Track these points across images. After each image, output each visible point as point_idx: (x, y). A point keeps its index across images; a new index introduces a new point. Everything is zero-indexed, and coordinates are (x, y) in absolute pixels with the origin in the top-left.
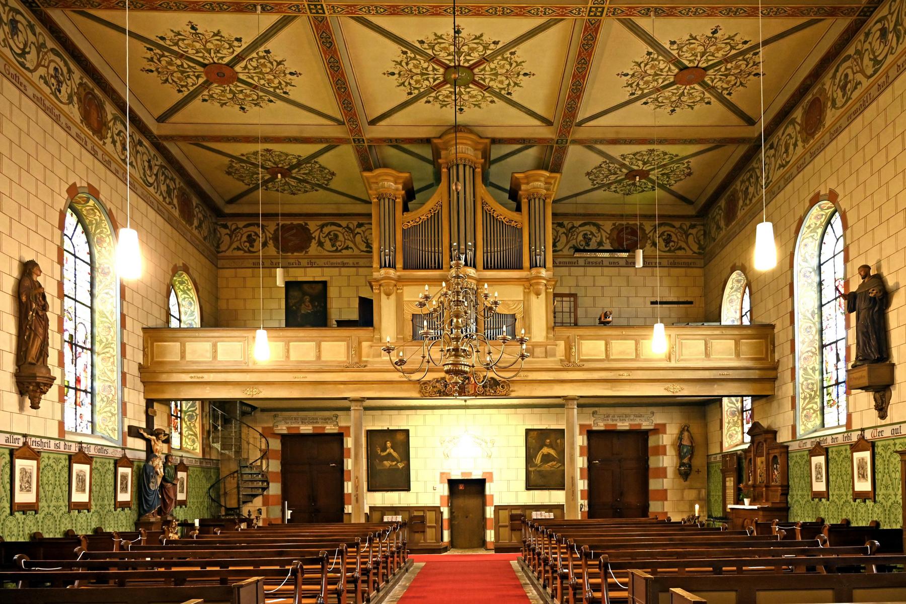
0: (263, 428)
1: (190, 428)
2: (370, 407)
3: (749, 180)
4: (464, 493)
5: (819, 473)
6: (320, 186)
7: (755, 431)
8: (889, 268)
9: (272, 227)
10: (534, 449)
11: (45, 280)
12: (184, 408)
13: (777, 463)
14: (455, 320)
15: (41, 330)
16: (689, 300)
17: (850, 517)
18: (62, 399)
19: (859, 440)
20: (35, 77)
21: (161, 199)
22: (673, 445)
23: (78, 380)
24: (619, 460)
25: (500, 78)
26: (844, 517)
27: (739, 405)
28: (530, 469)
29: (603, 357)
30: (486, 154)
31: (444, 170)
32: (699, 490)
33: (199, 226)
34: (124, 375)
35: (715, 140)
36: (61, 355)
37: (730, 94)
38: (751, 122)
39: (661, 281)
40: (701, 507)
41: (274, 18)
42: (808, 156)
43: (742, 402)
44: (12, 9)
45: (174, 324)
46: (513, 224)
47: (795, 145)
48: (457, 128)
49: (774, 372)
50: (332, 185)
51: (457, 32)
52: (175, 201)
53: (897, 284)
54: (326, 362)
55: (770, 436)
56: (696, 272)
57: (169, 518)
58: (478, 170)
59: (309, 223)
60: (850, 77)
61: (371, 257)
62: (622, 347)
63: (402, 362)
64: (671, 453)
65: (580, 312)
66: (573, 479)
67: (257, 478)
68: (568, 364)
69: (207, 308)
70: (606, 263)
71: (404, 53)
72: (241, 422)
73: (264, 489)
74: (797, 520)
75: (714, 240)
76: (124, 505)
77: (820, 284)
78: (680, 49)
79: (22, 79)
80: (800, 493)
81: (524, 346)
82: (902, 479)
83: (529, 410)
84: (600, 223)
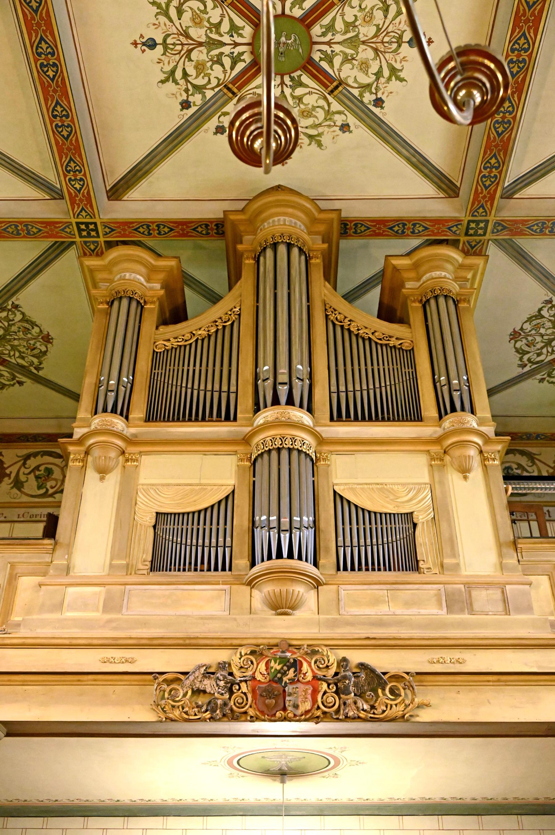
31: (249, 262)
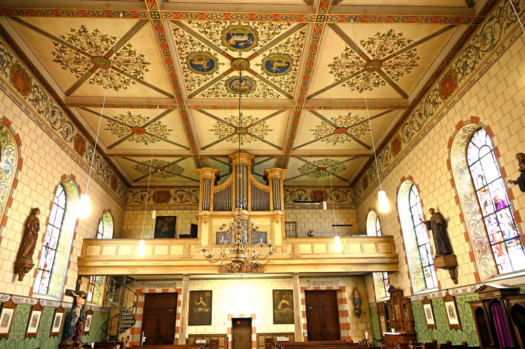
0: (136, 290)
1: (98, 290)
2: (192, 278)
3: (371, 171)
4: (241, 326)
5: (429, 314)
6: (177, 174)
7: (392, 290)
8: (443, 210)
9: (153, 192)
10: (277, 301)
11: (41, 217)
12: (97, 280)
13: (406, 308)
14: (237, 236)
15: (33, 241)
16: (350, 224)
17: (450, 340)
18: (35, 276)
19: (446, 295)
20: (58, 132)
21: (103, 180)
22: (350, 298)
23: (45, 266)
24: (322, 305)
25: (259, 132)
26: (447, 340)
27: (382, 276)
28: (276, 312)
29: (310, 252)
30: (253, 161)
32: (367, 323)
33: (119, 191)
34: (69, 262)
35: (354, 155)
36: (40, 252)
37: (359, 137)
38: (369, 148)
39: (336, 215)
40: (369, 334)
41: (164, 110)
42: (397, 161)
43: (383, 274)
44: (54, 107)
45: (99, 237)
46: (265, 191)
47: (390, 157)
48: (240, 151)
49: (397, 259)
50: (183, 174)
51: (241, 115)
52: (110, 181)
53: (449, 217)
54: (172, 255)
55: (400, 293)
56: (352, 211)
57: (78, 342)
58: (249, 168)
59: (170, 190)
60: (410, 131)
61: (198, 205)
62: (320, 247)
63: (210, 256)
64: (349, 302)
65: (298, 230)
66: (298, 317)
67: (129, 318)
68: (294, 256)
69: (117, 229)
70: (309, 207)
71: (218, 122)
72: (126, 287)
73: (132, 324)
74: (422, 341)
75: (359, 197)
76: (56, 334)
77: (412, 216)
78: (335, 121)
79: (52, 133)
80: (421, 325)
81: (271, 248)
82: (473, 317)
83: (274, 280)
84: (306, 189)
